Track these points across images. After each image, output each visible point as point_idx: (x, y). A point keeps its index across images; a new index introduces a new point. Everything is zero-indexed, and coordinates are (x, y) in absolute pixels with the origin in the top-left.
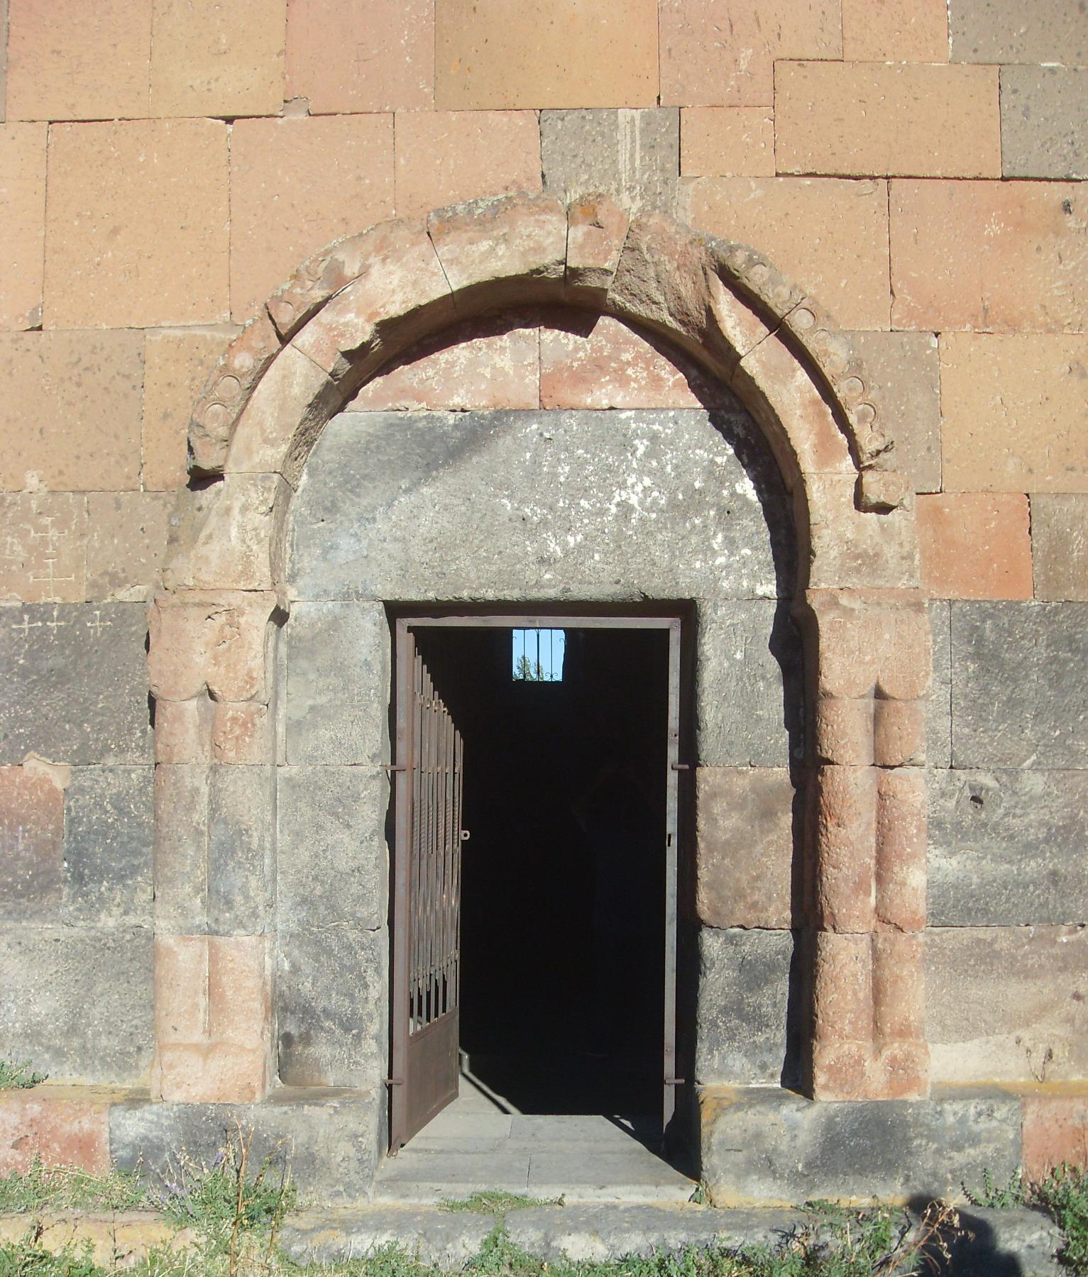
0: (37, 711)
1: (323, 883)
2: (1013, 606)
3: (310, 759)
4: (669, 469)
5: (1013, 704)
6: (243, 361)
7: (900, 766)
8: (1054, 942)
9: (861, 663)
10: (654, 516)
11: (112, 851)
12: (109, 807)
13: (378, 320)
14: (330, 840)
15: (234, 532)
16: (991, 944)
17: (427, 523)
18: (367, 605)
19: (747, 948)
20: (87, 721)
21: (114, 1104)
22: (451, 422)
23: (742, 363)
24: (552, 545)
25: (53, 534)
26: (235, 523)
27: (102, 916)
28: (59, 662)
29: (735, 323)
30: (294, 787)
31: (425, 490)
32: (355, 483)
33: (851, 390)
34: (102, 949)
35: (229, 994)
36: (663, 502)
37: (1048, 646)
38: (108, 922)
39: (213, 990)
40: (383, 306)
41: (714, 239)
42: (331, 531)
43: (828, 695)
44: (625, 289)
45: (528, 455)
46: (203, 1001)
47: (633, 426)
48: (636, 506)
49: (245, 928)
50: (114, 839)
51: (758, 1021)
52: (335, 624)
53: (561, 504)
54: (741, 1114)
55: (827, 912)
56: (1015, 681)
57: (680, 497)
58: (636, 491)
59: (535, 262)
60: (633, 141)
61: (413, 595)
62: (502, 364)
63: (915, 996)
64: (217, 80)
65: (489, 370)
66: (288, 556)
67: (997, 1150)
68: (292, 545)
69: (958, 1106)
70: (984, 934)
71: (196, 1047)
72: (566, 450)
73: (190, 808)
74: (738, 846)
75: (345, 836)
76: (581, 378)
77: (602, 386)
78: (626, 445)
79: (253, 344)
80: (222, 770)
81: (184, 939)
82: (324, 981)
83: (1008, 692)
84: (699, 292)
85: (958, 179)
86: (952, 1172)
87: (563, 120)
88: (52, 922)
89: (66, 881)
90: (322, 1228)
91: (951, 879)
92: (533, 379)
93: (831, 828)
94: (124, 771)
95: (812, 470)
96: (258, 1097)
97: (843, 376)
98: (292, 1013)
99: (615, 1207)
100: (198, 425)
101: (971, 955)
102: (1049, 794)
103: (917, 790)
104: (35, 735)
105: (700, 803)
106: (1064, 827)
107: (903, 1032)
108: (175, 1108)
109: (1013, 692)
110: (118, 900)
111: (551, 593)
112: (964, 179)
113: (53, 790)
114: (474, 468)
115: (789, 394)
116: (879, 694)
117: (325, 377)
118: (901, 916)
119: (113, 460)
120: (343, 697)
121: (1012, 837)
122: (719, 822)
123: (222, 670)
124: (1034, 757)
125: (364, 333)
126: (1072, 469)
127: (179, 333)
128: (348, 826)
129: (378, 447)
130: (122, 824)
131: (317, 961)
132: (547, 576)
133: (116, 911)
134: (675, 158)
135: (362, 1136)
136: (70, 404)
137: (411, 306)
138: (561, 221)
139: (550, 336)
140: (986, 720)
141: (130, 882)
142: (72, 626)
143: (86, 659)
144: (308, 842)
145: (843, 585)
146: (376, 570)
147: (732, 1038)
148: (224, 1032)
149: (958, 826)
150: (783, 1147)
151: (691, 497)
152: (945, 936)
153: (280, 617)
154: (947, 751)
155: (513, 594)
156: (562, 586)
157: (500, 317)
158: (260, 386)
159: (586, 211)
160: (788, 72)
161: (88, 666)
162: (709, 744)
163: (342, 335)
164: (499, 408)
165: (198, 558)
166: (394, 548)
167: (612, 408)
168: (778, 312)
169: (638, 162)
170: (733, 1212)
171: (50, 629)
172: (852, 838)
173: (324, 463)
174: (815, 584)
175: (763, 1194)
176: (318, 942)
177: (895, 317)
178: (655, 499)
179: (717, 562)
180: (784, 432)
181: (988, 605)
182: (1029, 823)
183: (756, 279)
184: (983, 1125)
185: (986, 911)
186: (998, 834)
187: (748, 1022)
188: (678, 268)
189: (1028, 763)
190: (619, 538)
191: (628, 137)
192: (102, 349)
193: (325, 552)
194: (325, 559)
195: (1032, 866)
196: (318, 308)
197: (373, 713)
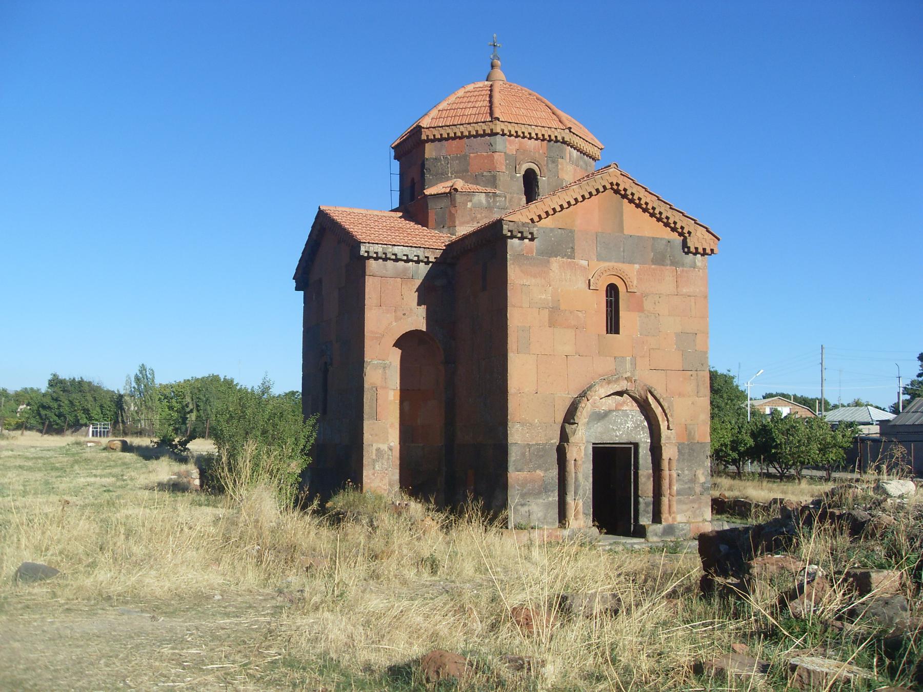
5: (683, 460)
17: (599, 430)
38: (550, 499)
51: (648, 513)
58: (630, 424)
63: (675, 507)
74: (645, 484)
76: (622, 405)
115: (658, 411)
139: (617, 397)
162: (641, 467)
175: (655, 539)
183: (655, 393)
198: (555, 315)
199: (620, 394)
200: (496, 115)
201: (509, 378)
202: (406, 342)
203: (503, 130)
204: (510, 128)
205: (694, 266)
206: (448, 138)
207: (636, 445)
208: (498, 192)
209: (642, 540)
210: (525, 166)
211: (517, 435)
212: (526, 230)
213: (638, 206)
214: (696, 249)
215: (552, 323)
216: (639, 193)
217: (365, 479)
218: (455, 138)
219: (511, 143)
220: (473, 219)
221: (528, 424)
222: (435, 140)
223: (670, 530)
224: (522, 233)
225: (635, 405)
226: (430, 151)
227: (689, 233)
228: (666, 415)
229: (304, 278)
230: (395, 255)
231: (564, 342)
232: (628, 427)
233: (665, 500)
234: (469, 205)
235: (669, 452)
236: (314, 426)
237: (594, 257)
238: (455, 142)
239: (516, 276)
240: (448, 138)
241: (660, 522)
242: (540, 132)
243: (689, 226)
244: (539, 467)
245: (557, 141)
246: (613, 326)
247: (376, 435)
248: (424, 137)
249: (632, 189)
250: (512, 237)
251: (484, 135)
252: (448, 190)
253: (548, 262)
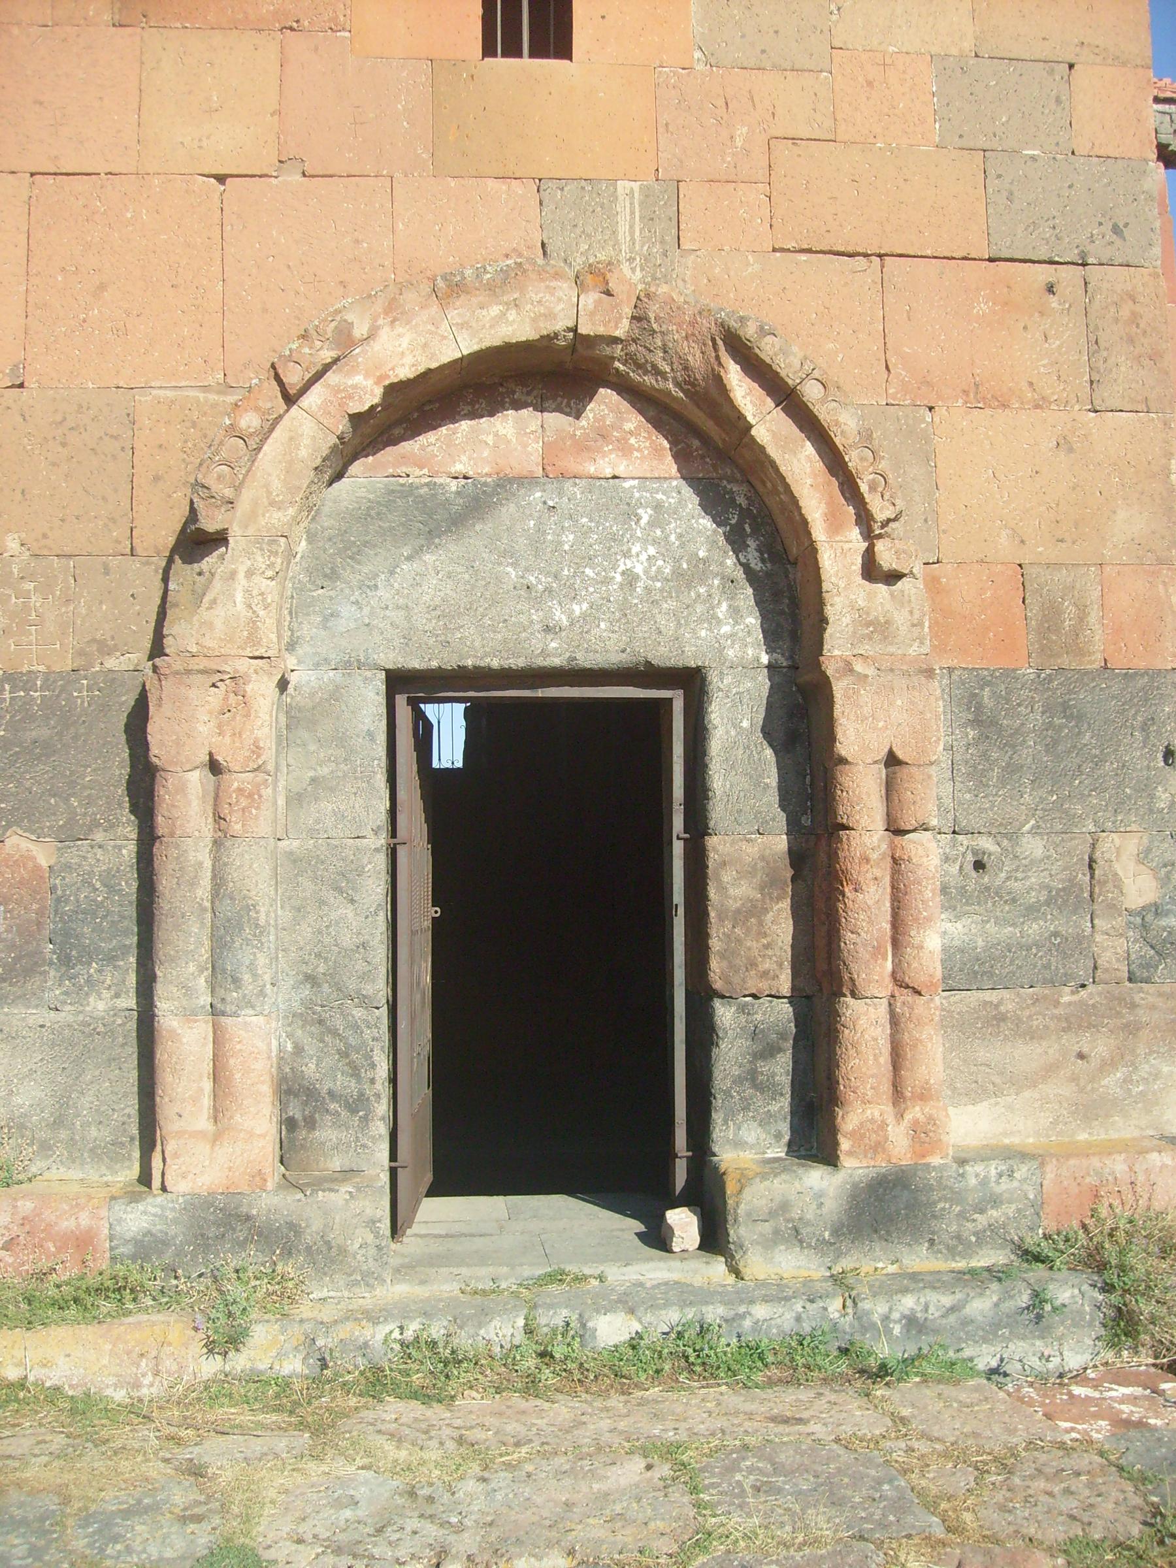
0: (19, 783)
1: (326, 959)
2: (1009, 674)
3: (312, 833)
4: (673, 538)
5: (1012, 769)
6: (250, 421)
7: (914, 830)
8: (1057, 1004)
9: (875, 729)
10: (658, 585)
11: (103, 931)
12: (98, 885)
13: (387, 382)
14: (334, 916)
15: (239, 597)
16: (997, 1006)
17: (432, 590)
18: (369, 674)
19: (759, 1017)
20: (74, 795)
21: (113, 1198)
22: (454, 489)
23: (753, 432)
24: (558, 614)
25: (36, 600)
26: (240, 588)
27: (91, 1000)
28: (44, 733)
29: (744, 392)
30: (295, 861)
31: (429, 558)
32: (355, 550)
33: (862, 459)
34: (91, 1035)
35: (238, 1076)
36: (667, 571)
37: (1043, 713)
38: (98, 1005)
39: (218, 1074)
40: (393, 369)
41: (722, 310)
42: (331, 598)
43: (843, 761)
44: (629, 359)
45: (532, 523)
46: (208, 1085)
47: (637, 495)
48: (641, 574)
49: (253, 1007)
50: (104, 917)
52: (336, 694)
53: (566, 572)
54: (767, 1183)
55: (846, 977)
56: (1013, 746)
57: (685, 566)
59: (546, 328)
60: (632, 213)
61: (416, 664)
62: (504, 432)
63: (933, 1057)
64: (208, 138)
65: (491, 437)
66: (287, 624)
67: (1019, 1210)
68: (290, 613)
69: (979, 1168)
70: (989, 996)
71: (201, 1134)
72: (571, 518)
73: (193, 884)
75: (349, 912)
76: (583, 447)
77: (604, 456)
78: (631, 515)
79: (260, 403)
80: (228, 843)
81: (189, 1021)
82: (328, 1062)
83: (1007, 758)
84: (708, 362)
85: (948, 258)
86: (976, 1234)
87: (562, 189)
88: (37, 1007)
89: (51, 964)
90: (347, 1319)
91: (956, 943)
92: (536, 447)
93: (848, 894)
94: (114, 847)
95: (824, 538)
96: (270, 1185)
97: (854, 446)
98: (296, 1096)
99: (641, 1284)
100: (203, 486)
101: (978, 1018)
102: (1048, 857)
103: (928, 854)
104: (18, 809)
105: (710, 872)
106: (1064, 889)
107: (924, 1096)
108: (181, 1200)
109: (1011, 758)
110: (108, 982)
111: (557, 662)
112: (954, 258)
113: (37, 868)
114: (476, 539)
116: (892, 760)
117: (333, 440)
118: (916, 977)
119: (101, 523)
120: (346, 768)
121: (1014, 900)
122: (730, 889)
123: (228, 740)
124: (1033, 822)
125: (372, 394)
126: (1062, 541)
127: (170, 394)
128: (352, 901)
129: (378, 514)
130: (113, 902)
131: (322, 1041)
132: (553, 645)
133: (106, 994)
134: (674, 231)
135: (380, 1221)
136: (54, 464)
137: (421, 369)
138: (571, 288)
140: (988, 786)
141: (122, 963)
142: (58, 696)
143: (72, 730)
144: (311, 918)
145: (855, 652)
146: (378, 639)
147: (745, 1109)
148: (231, 1117)
149: (962, 891)
150: (809, 1216)
151: (696, 566)
152: (952, 999)
153: (283, 685)
154: (951, 816)
155: (518, 663)
156: (568, 655)
157: (502, 385)
158: (265, 448)
159: (596, 278)
160: (783, 150)
161: (76, 738)
162: (718, 812)
163: (350, 397)
164: (501, 475)
165: (202, 624)
166: (398, 616)
167: (615, 477)
168: (790, 382)
169: (637, 233)
170: (761, 1284)
171: (33, 699)
172: (870, 902)
173: (324, 529)
174: (829, 651)
176: (321, 1022)
177: (891, 391)
178: (659, 568)
179: (722, 631)
180: (795, 501)
181: (986, 673)
182: (1030, 886)
184: (1005, 1185)
185: (991, 974)
186: (1001, 897)
187: (762, 1091)
188: (687, 337)
189: (1027, 827)
190: (625, 608)
191: (628, 209)
192: (88, 408)
193: (326, 619)
194: (325, 628)
195: (1034, 929)
196: (326, 368)
197: (376, 785)
223: (889, 1207)
241: (828, 1156)
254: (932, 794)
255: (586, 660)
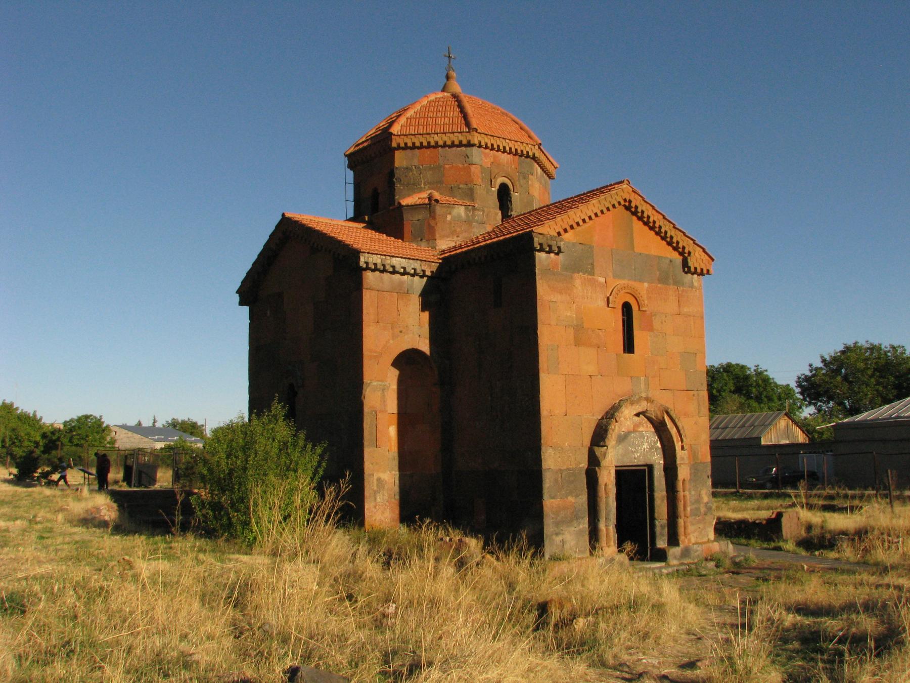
17: (621, 451)
38: (581, 526)
51: (663, 535)
58: (645, 446)
63: (690, 528)
115: (673, 431)
162: (656, 489)
183: (672, 413)
198: (580, 335)
199: (638, 415)
200: (475, 126)
201: (541, 399)
202: (407, 361)
203: (480, 143)
204: (486, 140)
205: (692, 286)
206: (421, 147)
207: (650, 467)
208: (477, 206)
209: (663, 564)
210: (500, 180)
211: (551, 460)
212: (553, 243)
213: (646, 224)
214: (696, 269)
215: (578, 342)
216: (648, 211)
217: (367, 513)
218: (429, 146)
219: (486, 156)
220: (454, 233)
221: (561, 450)
222: (406, 147)
223: (686, 553)
224: (550, 246)
225: (650, 425)
226: (400, 160)
227: (689, 253)
228: (680, 435)
229: (251, 292)
230: (393, 267)
231: (587, 361)
232: (644, 449)
233: (681, 522)
234: (449, 218)
235: (683, 472)
236: (321, 456)
237: (611, 274)
238: (428, 152)
239: (546, 292)
240: (421, 147)
241: (677, 545)
242: (514, 146)
243: (689, 247)
244: (571, 493)
245: (528, 156)
246: (629, 347)
247: (377, 464)
248: (394, 145)
249: (642, 207)
250: (539, 251)
251: (461, 145)
252: (427, 201)
253: (572, 278)
254: (687, 485)
255: (640, 463)
